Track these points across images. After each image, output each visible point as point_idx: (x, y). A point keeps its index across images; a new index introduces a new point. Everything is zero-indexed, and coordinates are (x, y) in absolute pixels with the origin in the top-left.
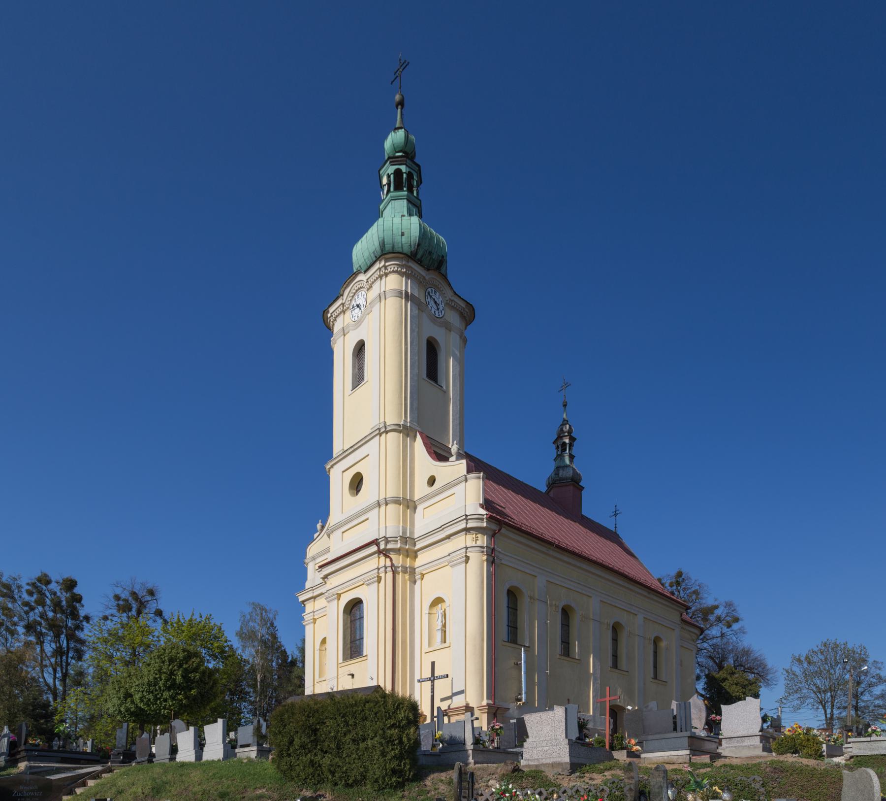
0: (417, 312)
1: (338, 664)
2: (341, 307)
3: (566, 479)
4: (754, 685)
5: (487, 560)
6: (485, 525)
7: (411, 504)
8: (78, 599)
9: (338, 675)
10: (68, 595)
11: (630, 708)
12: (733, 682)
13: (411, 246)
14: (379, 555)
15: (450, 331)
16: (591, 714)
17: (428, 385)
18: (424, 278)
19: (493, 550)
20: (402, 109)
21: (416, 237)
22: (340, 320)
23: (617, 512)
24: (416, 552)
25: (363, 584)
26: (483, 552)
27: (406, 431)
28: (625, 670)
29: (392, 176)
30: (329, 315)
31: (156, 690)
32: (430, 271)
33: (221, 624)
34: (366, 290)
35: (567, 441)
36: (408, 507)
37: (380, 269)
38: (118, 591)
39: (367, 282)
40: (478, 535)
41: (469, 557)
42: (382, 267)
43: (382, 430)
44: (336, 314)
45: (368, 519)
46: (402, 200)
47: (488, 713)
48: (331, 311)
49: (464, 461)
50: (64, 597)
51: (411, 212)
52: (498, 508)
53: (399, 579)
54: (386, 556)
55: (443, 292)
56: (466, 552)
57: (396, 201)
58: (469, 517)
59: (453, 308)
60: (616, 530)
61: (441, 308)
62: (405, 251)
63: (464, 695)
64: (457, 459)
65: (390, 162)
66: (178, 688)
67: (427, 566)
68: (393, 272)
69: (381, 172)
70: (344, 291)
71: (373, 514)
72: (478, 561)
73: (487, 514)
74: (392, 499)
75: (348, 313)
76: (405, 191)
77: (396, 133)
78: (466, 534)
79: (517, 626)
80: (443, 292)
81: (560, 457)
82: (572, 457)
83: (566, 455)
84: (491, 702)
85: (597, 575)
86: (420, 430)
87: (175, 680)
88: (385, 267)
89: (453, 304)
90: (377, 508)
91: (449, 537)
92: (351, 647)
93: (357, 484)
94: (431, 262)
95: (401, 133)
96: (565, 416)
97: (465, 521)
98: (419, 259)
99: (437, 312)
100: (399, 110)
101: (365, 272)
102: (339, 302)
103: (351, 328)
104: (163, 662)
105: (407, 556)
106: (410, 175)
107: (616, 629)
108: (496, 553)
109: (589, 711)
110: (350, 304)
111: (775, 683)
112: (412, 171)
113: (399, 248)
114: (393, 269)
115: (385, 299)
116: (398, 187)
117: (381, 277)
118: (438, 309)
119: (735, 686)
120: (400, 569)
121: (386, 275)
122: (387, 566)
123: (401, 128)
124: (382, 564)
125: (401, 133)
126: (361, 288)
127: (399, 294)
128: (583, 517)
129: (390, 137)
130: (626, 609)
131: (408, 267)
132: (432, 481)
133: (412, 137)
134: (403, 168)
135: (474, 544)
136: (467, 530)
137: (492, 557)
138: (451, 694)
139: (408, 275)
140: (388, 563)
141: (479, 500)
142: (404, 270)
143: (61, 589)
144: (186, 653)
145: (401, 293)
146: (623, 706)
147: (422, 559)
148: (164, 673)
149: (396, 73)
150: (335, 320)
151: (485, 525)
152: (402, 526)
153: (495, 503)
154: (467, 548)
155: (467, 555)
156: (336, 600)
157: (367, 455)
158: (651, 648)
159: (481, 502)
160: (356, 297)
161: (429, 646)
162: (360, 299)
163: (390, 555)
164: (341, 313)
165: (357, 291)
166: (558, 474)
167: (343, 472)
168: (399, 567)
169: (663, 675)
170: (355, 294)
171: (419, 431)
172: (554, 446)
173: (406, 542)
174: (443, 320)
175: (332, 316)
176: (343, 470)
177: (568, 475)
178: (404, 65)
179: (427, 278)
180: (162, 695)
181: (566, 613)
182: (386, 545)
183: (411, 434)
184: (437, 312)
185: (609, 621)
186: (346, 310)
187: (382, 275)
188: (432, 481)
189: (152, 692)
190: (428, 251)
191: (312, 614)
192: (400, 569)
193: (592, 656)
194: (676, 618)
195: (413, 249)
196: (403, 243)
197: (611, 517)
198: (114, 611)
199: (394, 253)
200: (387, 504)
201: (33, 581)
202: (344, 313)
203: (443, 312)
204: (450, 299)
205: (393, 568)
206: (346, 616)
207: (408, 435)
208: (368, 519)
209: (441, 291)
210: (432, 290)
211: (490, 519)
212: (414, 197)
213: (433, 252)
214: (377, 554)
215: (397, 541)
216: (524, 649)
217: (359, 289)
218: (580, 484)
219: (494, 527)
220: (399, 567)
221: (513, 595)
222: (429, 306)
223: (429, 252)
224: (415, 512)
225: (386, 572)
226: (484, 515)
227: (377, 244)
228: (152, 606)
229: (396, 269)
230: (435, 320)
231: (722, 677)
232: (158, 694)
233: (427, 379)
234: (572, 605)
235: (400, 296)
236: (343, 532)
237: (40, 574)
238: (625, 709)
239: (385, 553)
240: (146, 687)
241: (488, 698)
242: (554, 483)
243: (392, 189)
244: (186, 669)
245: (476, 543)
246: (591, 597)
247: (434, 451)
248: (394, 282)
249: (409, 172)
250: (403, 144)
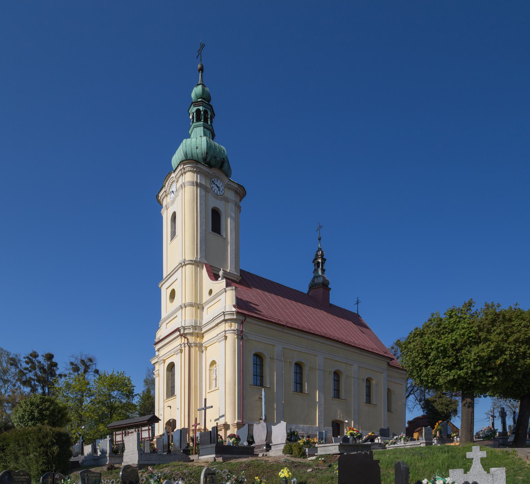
0: (204, 193)
1: (164, 401)
2: (165, 193)
3: (319, 284)
4: (454, 404)
5: (237, 338)
6: (235, 317)
7: (200, 306)
8: (56, 365)
9: (164, 407)
10: (49, 363)
11: (346, 421)
12: (439, 403)
13: (202, 154)
14: (181, 337)
15: (228, 202)
16: (317, 426)
17: (214, 236)
18: (208, 173)
19: (242, 331)
20: (202, 73)
22: (165, 200)
23: (359, 302)
24: (203, 334)
25: (174, 354)
26: (235, 333)
27: (196, 263)
28: (343, 398)
29: (195, 114)
30: (160, 198)
31: (24, 421)
32: (213, 169)
33: (129, 377)
34: (175, 182)
35: (320, 261)
36: (198, 308)
37: (181, 170)
38: (73, 360)
39: (176, 178)
40: (232, 323)
41: (227, 336)
42: (182, 169)
43: (183, 264)
44: (163, 197)
45: (177, 316)
47: (237, 427)
48: (160, 196)
49: (224, 280)
50: (46, 364)
51: (206, 133)
52: (252, 307)
53: (192, 350)
54: (185, 338)
55: (223, 180)
56: (225, 334)
57: (197, 128)
58: (225, 313)
59: (230, 189)
60: (358, 312)
61: (222, 189)
62: (195, 159)
63: (224, 417)
64: (222, 279)
65: (193, 105)
66: (37, 420)
67: (212, 343)
68: (189, 171)
69: (189, 112)
70: (165, 184)
71: (179, 313)
72: (232, 338)
73: (235, 311)
75: (169, 196)
78: (225, 323)
79: (263, 375)
80: (223, 180)
81: (316, 271)
82: (323, 271)
83: (319, 269)
84: (240, 421)
85: (321, 343)
86: (206, 262)
87: (34, 415)
88: (184, 169)
90: (181, 310)
91: (217, 325)
92: (171, 391)
93: (173, 295)
94: (216, 163)
95: (200, 88)
96: (319, 246)
97: (223, 315)
98: (208, 162)
99: (218, 192)
100: (200, 74)
101: (174, 172)
102: (163, 190)
103: (170, 205)
104: (28, 405)
105: (198, 337)
106: (205, 112)
107: (337, 375)
108: (244, 333)
109: (316, 424)
110: (169, 191)
111: (477, 402)
112: (206, 109)
113: (195, 156)
114: (188, 169)
115: (185, 187)
116: (198, 120)
117: (182, 174)
118: (219, 190)
119: (440, 405)
120: (193, 345)
121: (185, 173)
122: (185, 343)
123: (200, 84)
124: (183, 341)
125: (200, 88)
126: (173, 182)
127: (192, 184)
128: (331, 305)
129: (194, 90)
130: (345, 362)
131: (197, 168)
132: (211, 292)
133: (207, 89)
134: (201, 108)
135: (230, 329)
136: (225, 321)
137: (241, 336)
138: (219, 417)
139: (198, 172)
140: (186, 342)
142: (195, 169)
143: (45, 360)
144: (41, 400)
145: (193, 183)
146: (342, 420)
147: (207, 337)
148: (28, 411)
149: (199, 51)
150: (163, 201)
151: (235, 317)
152: (194, 320)
153: (251, 303)
154: (225, 331)
155: (226, 335)
156: (163, 364)
157: (176, 279)
158: (364, 385)
159: (234, 304)
160: (172, 187)
161: (210, 388)
162: (174, 189)
163: (187, 337)
164: (165, 196)
165: (172, 183)
166: (314, 281)
167: (167, 289)
168: (192, 344)
169: (374, 400)
170: (171, 185)
171: (205, 263)
172: (313, 264)
173: (196, 329)
174: (222, 197)
175: (161, 198)
176: (167, 288)
177: (320, 282)
178: (203, 46)
179: (210, 173)
180: (28, 424)
181: (299, 366)
182: (184, 331)
183: (200, 265)
184: (218, 192)
185: (331, 370)
186: (167, 194)
187: (183, 174)
188: (211, 292)
189: (22, 422)
191: (158, 371)
192: (193, 345)
193: (318, 391)
194: (384, 365)
195: (204, 156)
197: (355, 304)
198: (71, 371)
199: (188, 160)
200: (186, 307)
201: (27, 356)
202: (167, 196)
205: (189, 344)
206: (168, 372)
207: (198, 266)
208: (177, 316)
211: (238, 313)
212: (208, 126)
214: (180, 337)
215: (190, 328)
216: (264, 389)
217: (173, 182)
218: (329, 287)
220: (192, 344)
221: (259, 358)
224: (203, 311)
225: (185, 347)
226: (234, 312)
227: (183, 155)
228: (93, 368)
229: (190, 169)
230: (216, 196)
231: (433, 400)
232: (26, 423)
233: (212, 232)
234: (303, 362)
235: (193, 185)
236: (167, 324)
237: (32, 352)
238: (344, 422)
239: (184, 335)
240: (18, 420)
241: (238, 419)
242: (313, 286)
243: (195, 121)
244: (41, 409)
245: (231, 328)
246: (317, 356)
247: (214, 273)
248: (189, 177)
249: (205, 110)
250: (201, 94)
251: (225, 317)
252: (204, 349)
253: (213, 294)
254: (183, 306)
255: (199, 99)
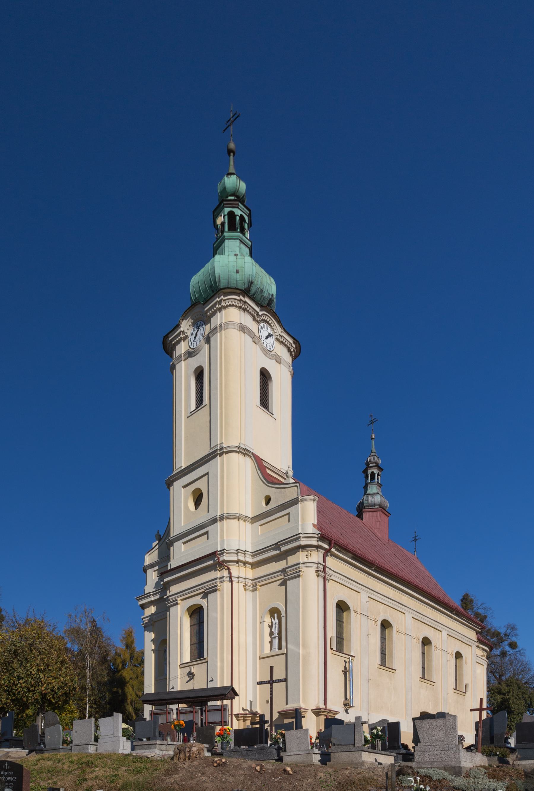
21: (250, 275)
46: (235, 240)
76: (238, 232)
77: (229, 178)
89: (282, 340)
100: (232, 157)
113: (234, 284)
123: (233, 174)
149: (228, 122)
179: (261, 313)
190: (260, 289)
196: (238, 280)
203: (274, 346)
204: (280, 335)
210: (264, 325)
213: (264, 290)
222: (262, 340)
223: (261, 290)
249: (241, 215)
253: (272, 505)
255: (231, 195)
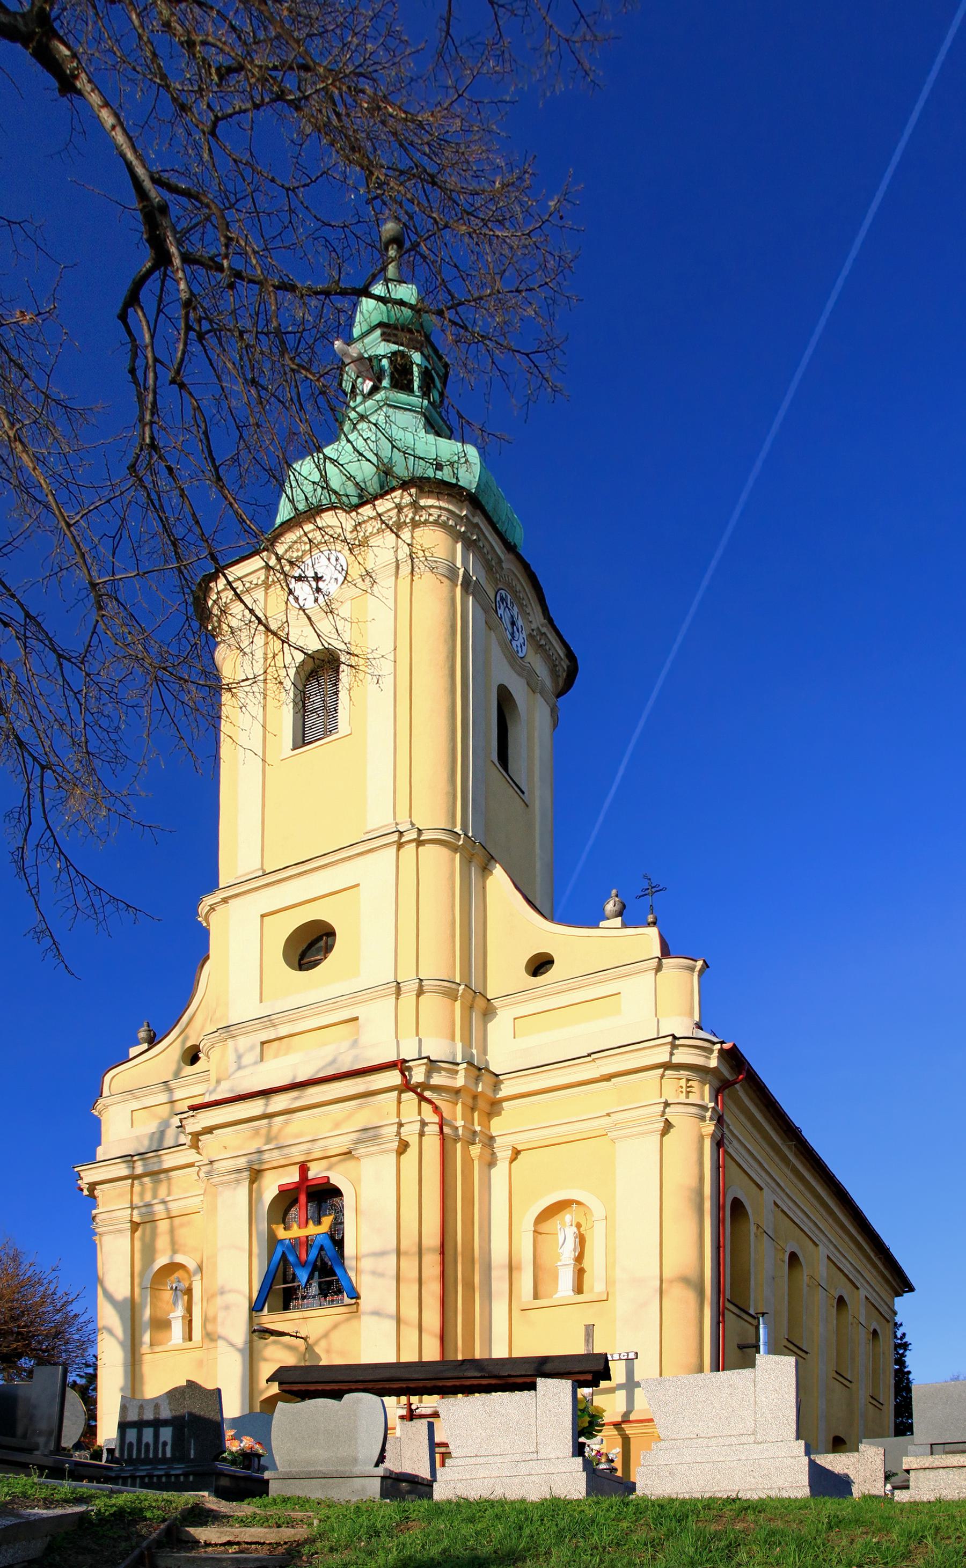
74: (448, 984)
89: (543, 642)
135: (682, 1098)
141: (691, 1014)
204: (538, 628)
209: (522, 605)
219: (727, 1073)
245: (687, 1097)
251: (672, 1054)
252: (503, 1155)
254: (410, 988)
